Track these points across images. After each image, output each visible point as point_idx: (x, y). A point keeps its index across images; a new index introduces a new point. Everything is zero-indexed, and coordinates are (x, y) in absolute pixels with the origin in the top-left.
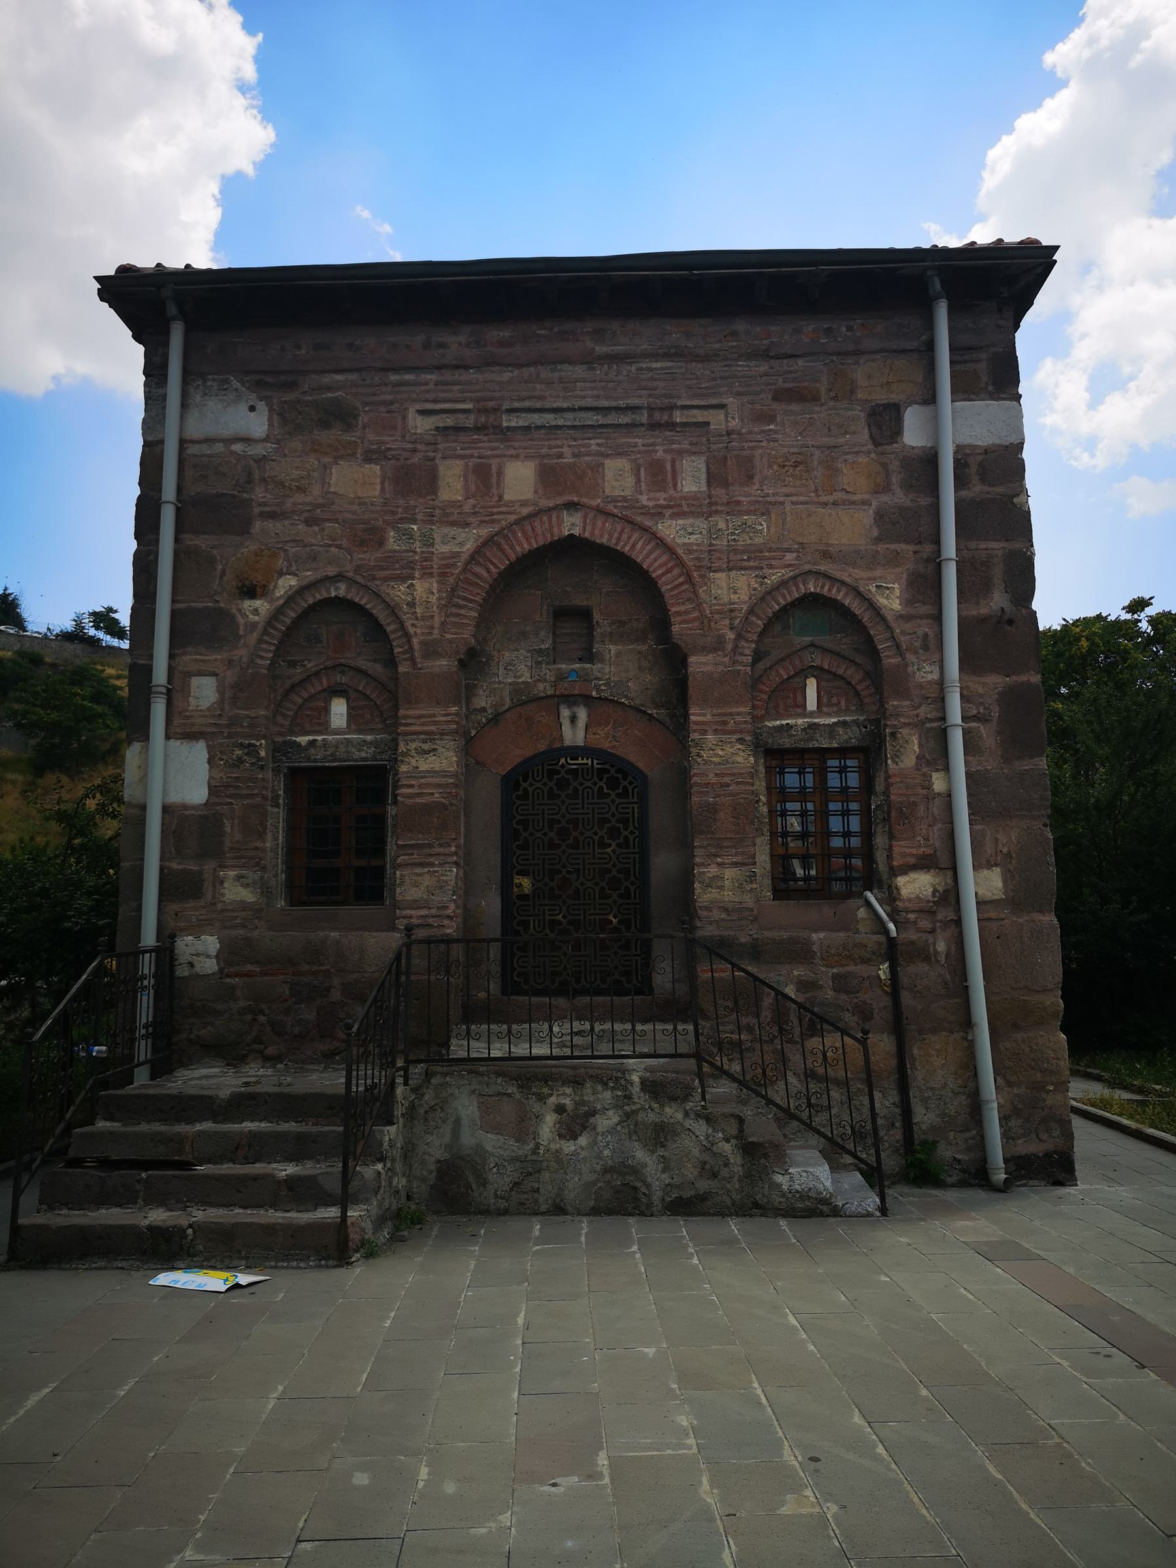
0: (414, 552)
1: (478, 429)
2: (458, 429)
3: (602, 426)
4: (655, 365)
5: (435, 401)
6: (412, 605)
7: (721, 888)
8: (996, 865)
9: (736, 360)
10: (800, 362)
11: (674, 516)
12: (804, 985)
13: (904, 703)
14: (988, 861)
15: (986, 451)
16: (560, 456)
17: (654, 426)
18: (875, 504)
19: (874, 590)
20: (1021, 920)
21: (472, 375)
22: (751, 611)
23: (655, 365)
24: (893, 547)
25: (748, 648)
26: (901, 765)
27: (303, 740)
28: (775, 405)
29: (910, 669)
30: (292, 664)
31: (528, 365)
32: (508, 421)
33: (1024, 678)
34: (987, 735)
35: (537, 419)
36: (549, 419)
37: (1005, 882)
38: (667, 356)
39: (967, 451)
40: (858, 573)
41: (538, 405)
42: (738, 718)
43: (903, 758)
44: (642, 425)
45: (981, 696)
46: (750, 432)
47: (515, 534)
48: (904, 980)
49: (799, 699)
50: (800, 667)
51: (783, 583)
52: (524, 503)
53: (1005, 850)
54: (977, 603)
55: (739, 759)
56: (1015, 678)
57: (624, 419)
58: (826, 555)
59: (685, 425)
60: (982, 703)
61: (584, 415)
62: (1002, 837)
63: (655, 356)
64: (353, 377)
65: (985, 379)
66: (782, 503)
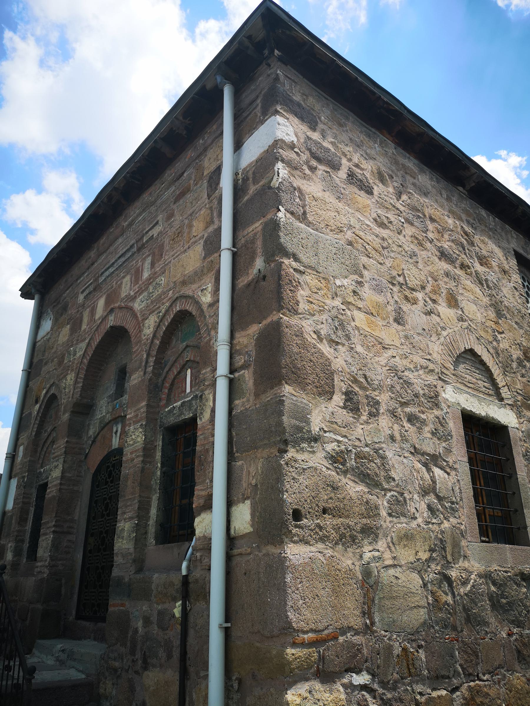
0: (70, 361)
1: (95, 289)
2: (90, 293)
3: (124, 262)
4: (140, 218)
5: (85, 284)
6: (65, 388)
7: (123, 538)
8: (248, 498)
9: (164, 193)
10: (185, 175)
11: (140, 294)
12: (147, 621)
13: (208, 369)
14: (243, 495)
15: (257, 161)
16: (112, 287)
17: (139, 250)
18: (206, 235)
19: (200, 293)
20: (260, 554)
21: (96, 265)
22: (154, 336)
23: (140, 218)
24: (209, 260)
25: (152, 360)
26: (203, 420)
27: (42, 470)
28: (175, 207)
29: (211, 343)
30: (46, 431)
31: (107, 250)
32: (101, 280)
33: (269, 320)
34: (247, 377)
35: (107, 273)
36: (111, 270)
37: (253, 515)
38: (144, 210)
39: (248, 169)
40: (194, 287)
41: (107, 266)
42: (142, 410)
43: (204, 414)
44: (135, 252)
45: (246, 346)
46: (164, 229)
47: (95, 335)
48: (191, 619)
49: (184, 386)
50: (182, 364)
51: (167, 311)
52: (99, 319)
53: (254, 482)
54: (248, 273)
55: (139, 439)
56: (265, 322)
57: (130, 253)
58: (184, 283)
59: (147, 241)
60: (247, 352)
61: (119, 261)
62: (252, 470)
63: (140, 214)
64: (70, 289)
65: (259, 115)
66: (170, 262)
